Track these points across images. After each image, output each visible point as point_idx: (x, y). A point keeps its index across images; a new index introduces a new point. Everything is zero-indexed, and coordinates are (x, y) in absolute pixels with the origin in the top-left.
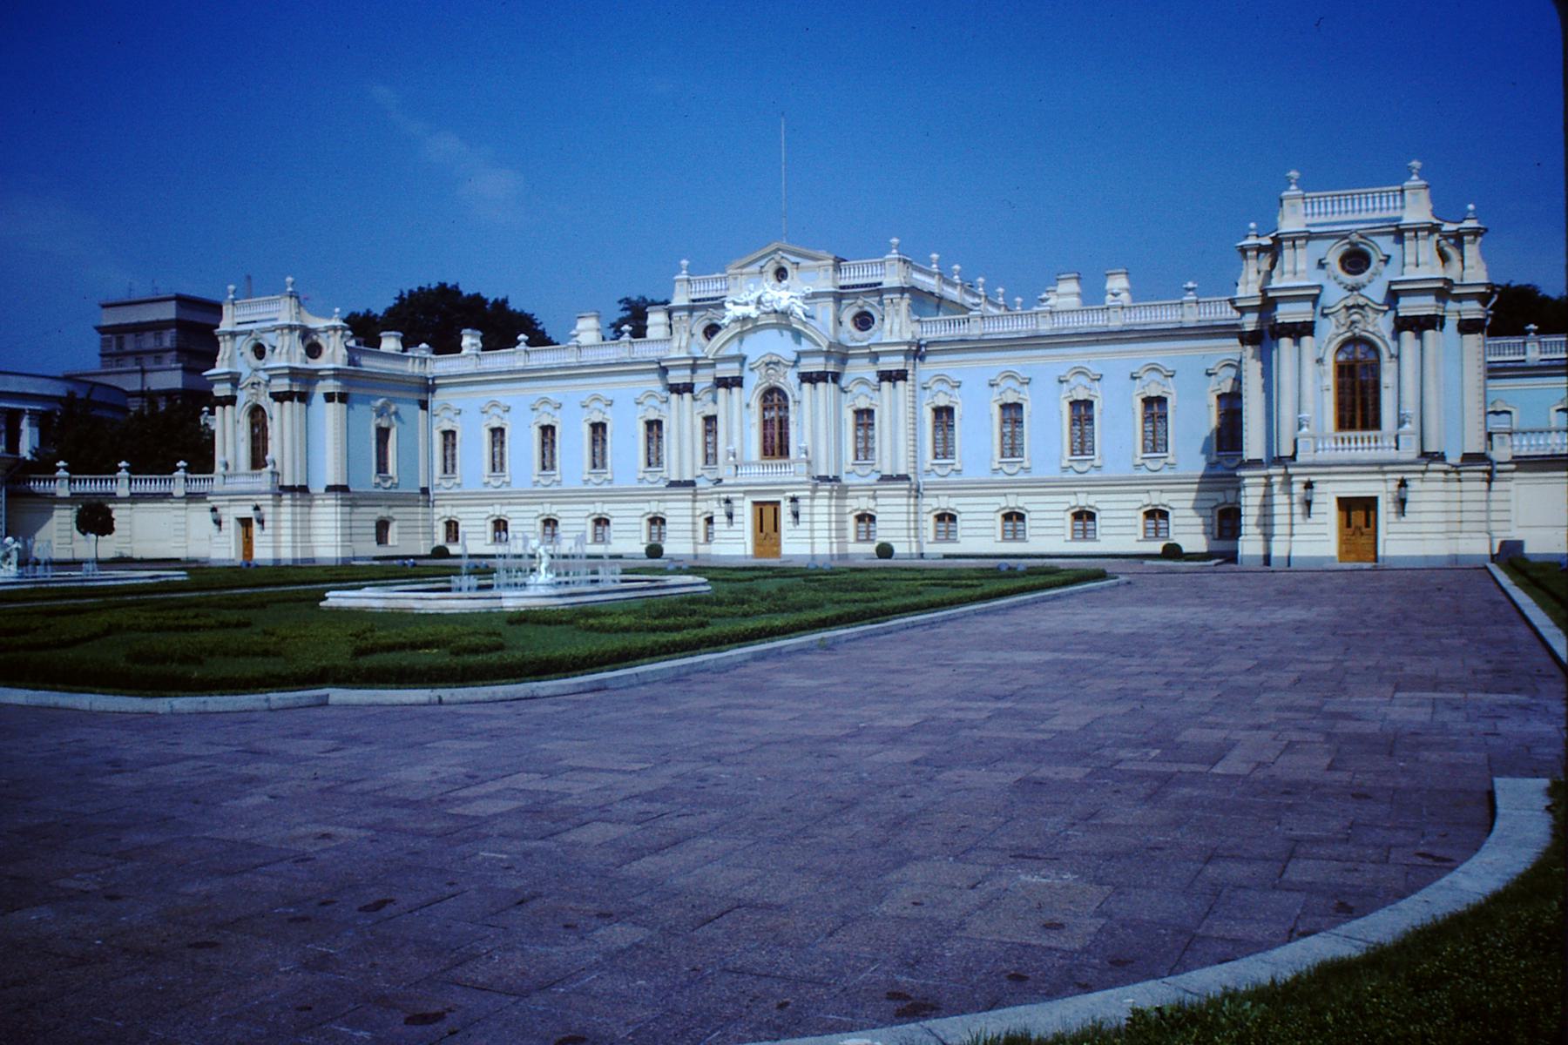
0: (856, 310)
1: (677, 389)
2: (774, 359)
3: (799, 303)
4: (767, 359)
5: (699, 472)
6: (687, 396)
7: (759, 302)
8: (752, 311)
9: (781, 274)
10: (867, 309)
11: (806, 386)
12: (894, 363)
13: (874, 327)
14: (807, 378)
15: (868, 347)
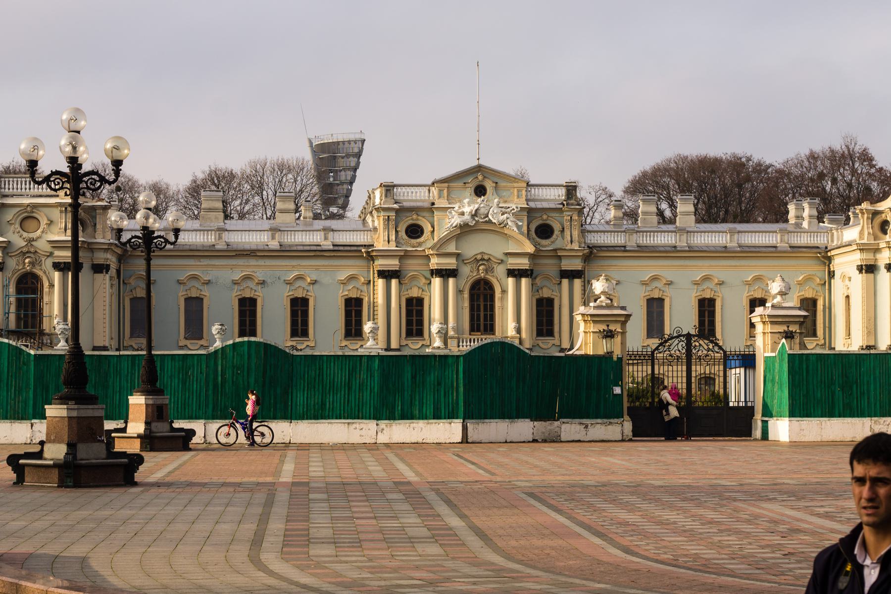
0: (541, 222)
1: (386, 275)
2: (486, 257)
3: (512, 218)
4: (479, 257)
5: (404, 343)
6: (394, 282)
7: (475, 215)
8: (467, 217)
9: (480, 191)
10: (548, 222)
11: (511, 281)
12: (576, 265)
13: (554, 236)
14: (511, 273)
15: (555, 250)
